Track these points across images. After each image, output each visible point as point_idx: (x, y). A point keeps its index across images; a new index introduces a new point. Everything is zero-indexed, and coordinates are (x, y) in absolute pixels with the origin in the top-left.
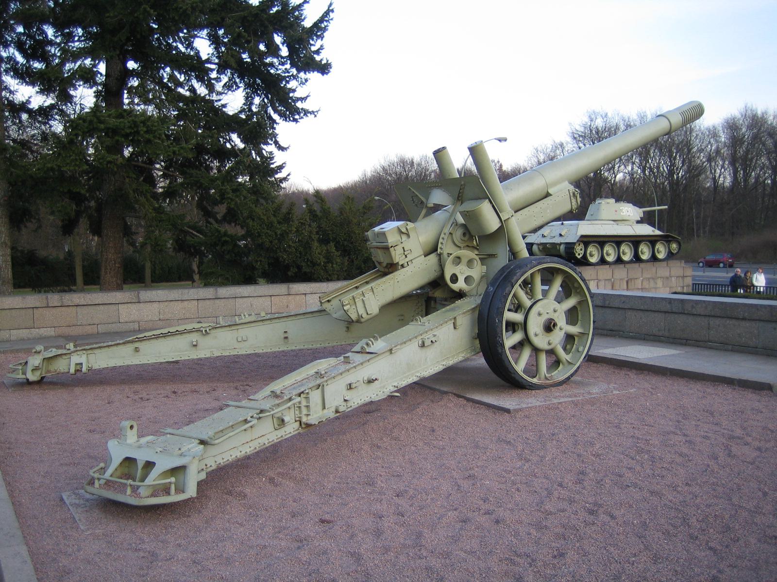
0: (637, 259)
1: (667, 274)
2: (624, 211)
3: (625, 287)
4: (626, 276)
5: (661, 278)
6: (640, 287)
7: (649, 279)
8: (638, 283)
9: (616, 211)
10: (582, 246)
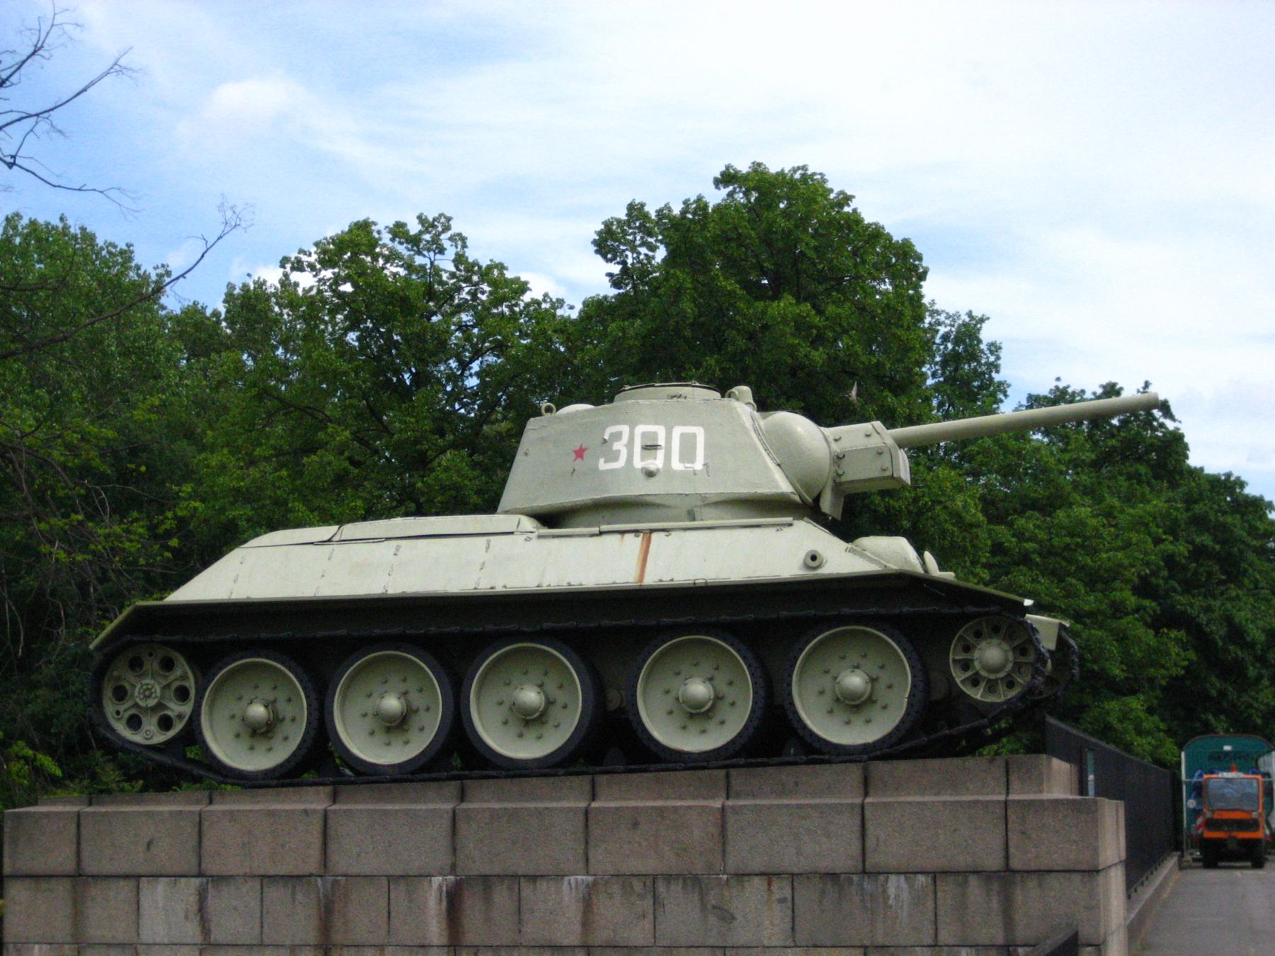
0: (611, 745)
2: (616, 446)
3: (435, 931)
4: (443, 859)
5: (769, 876)
9: (580, 453)
10: (183, 671)
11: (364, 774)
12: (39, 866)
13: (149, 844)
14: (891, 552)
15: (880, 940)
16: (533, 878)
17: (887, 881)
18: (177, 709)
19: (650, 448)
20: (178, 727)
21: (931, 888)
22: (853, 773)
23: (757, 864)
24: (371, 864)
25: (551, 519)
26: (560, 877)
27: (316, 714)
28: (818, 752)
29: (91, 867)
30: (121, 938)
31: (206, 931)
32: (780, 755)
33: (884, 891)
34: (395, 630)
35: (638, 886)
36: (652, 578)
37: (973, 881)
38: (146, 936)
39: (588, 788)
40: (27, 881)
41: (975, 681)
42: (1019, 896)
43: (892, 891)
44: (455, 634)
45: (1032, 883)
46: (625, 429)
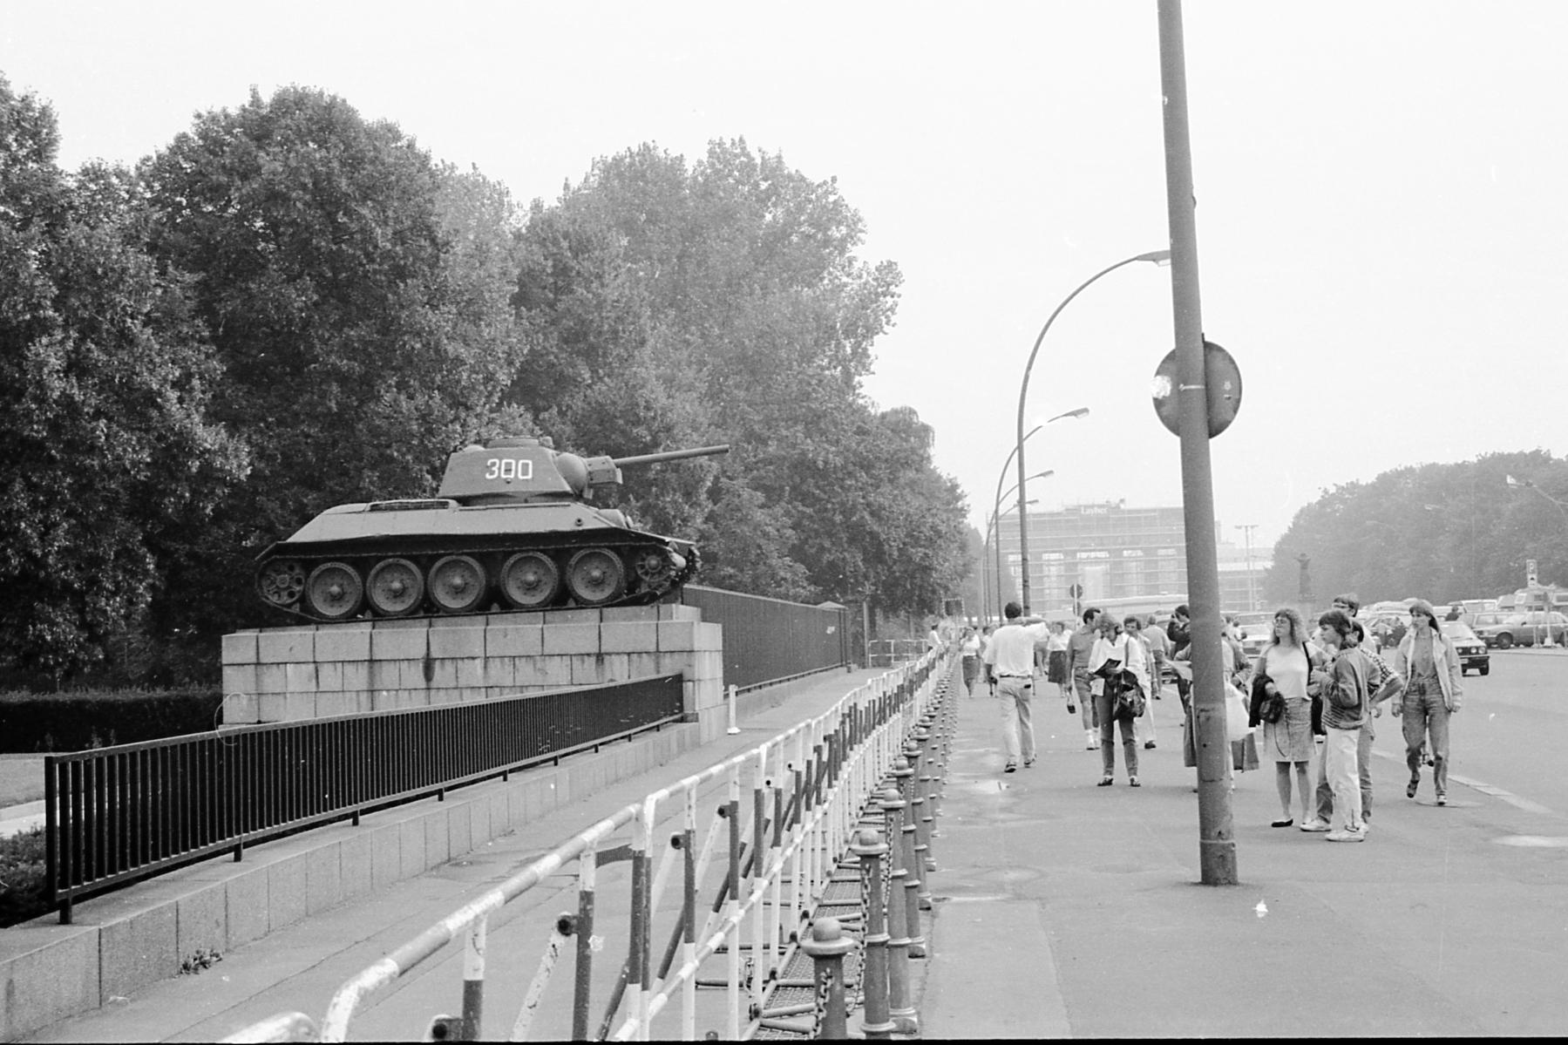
19: (508, 471)
22: (596, 613)
25: (464, 501)
29: (263, 660)
41: (646, 573)
44: (425, 551)
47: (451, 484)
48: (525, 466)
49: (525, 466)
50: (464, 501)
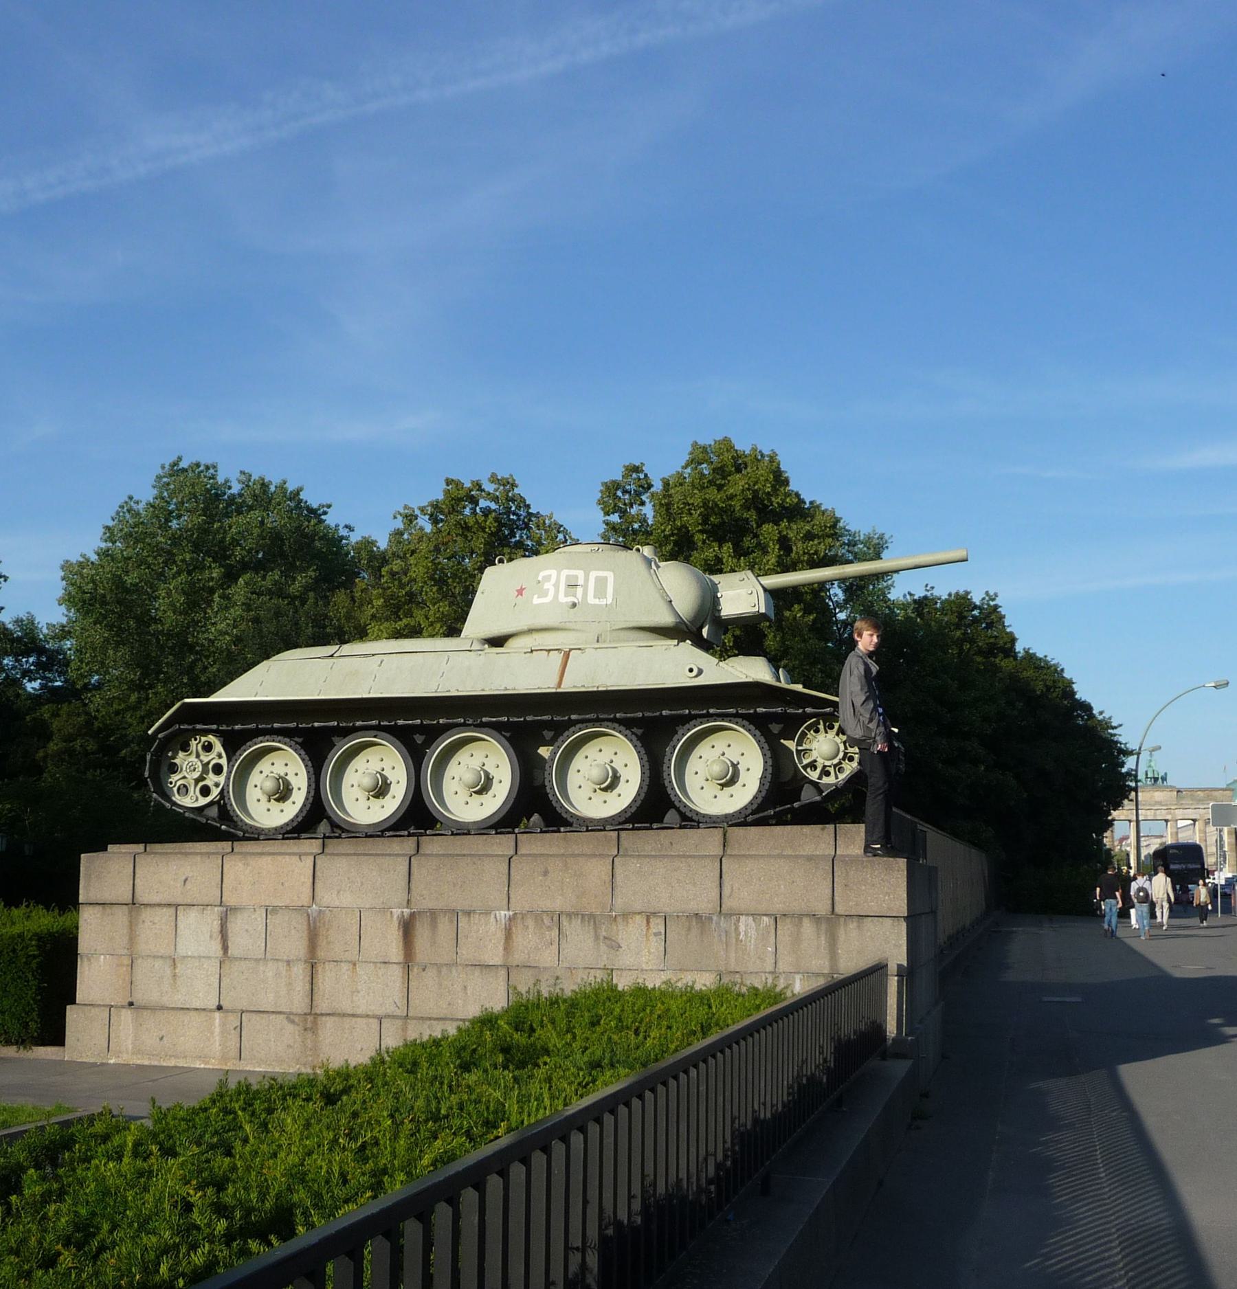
1: (702, 898)
2: (547, 586)
3: (395, 951)
6: (497, 960)
7: (558, 918)
8: (485, 937)
9: (520, 592)
11: (348, 831)
12: (107, 896)
13: (186, 880)
14: (752, 670)
15: (732, 967)
16: (468, 913)
17: (738, 921)
18: (211, 779)
20: (215, 792)
21: (773, 927)
22: (717, 834)
23: (638, 907)
24: (346, 900)
26: (487, 913)
27: (313, 786)
28: (690, 820)
30: (162, 952)
31: (225, 948)
32: (661, 821)
33: (737, 929)
34: (374, 722)
35: (547, 921)
36: (568, 686)
37: (806, 921)
38: (182, 950)
39: (513, 844)
40: (97, 907)
42: (842, 934)
43: (742, 928)
44: (420, 726)
45: (853, 925)
46: (554, 573)
47: (485, 615)
48: (601, 582)
49: (601, 582)
50: (497, 642)
